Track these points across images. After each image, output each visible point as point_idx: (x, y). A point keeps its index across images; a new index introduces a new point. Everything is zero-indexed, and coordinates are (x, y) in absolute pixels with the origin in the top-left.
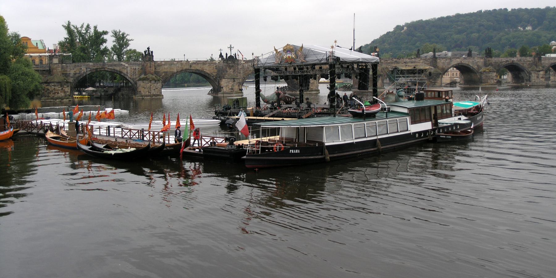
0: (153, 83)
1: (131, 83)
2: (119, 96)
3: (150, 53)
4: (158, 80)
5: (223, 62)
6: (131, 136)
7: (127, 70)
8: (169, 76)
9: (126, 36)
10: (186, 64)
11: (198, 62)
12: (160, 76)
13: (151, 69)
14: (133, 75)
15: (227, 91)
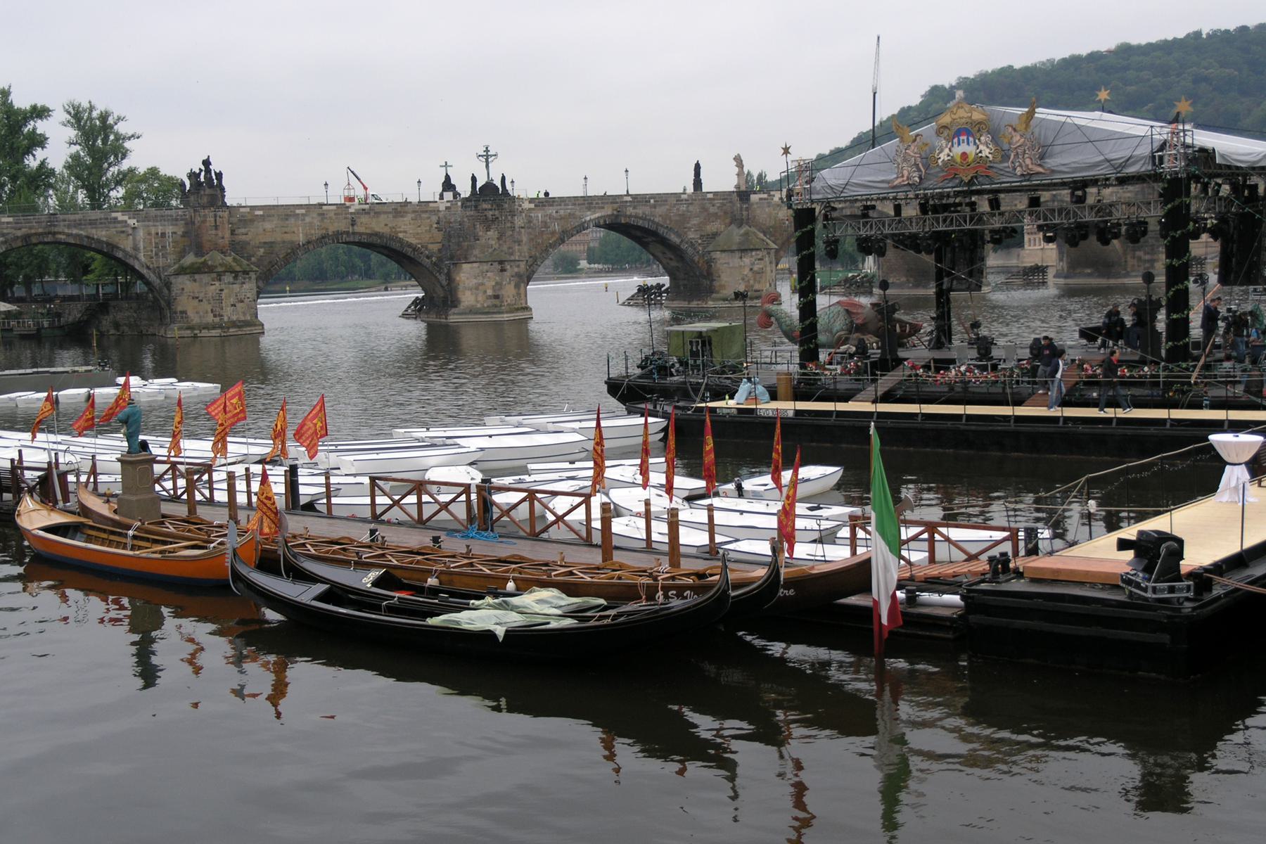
0: (229, 283)
1: (147, 283)
2: (104, 329)
3: (214, 177)
4: (246, 272)
5: (462, 205)
6: (206, 477)
7: (134, 239)
8: (281, 256)
9: (116, 124)
10: (335, 214)
11: (378, 208)
12: (248, 259)
13: (220, 234)
14: (156, 254)
15: (479, 306)
